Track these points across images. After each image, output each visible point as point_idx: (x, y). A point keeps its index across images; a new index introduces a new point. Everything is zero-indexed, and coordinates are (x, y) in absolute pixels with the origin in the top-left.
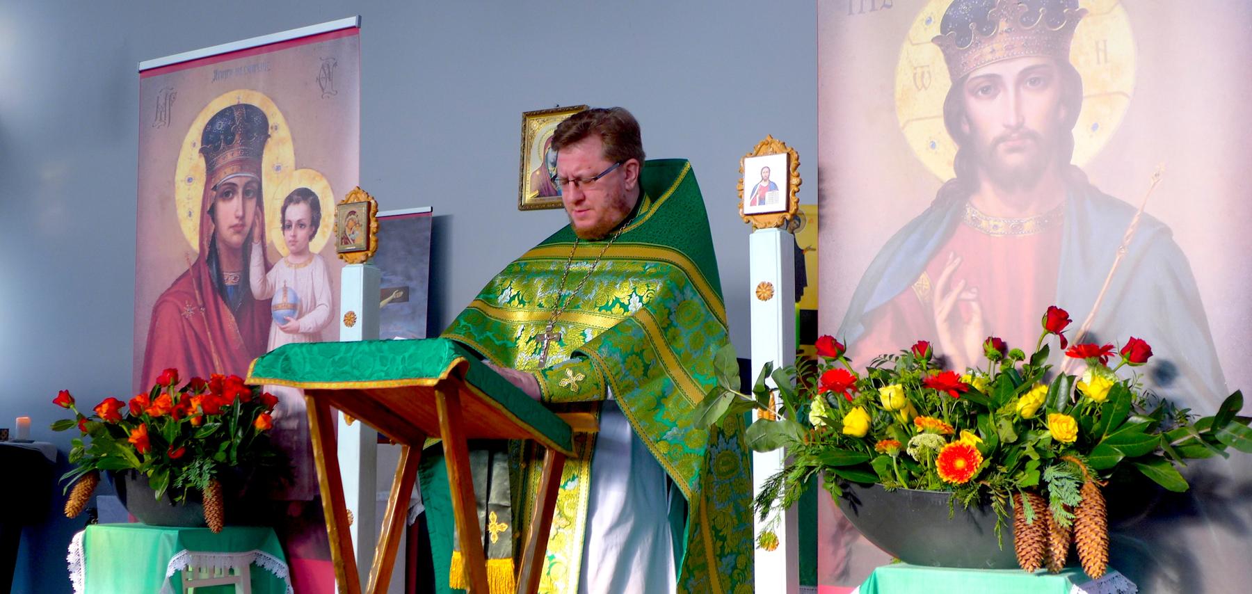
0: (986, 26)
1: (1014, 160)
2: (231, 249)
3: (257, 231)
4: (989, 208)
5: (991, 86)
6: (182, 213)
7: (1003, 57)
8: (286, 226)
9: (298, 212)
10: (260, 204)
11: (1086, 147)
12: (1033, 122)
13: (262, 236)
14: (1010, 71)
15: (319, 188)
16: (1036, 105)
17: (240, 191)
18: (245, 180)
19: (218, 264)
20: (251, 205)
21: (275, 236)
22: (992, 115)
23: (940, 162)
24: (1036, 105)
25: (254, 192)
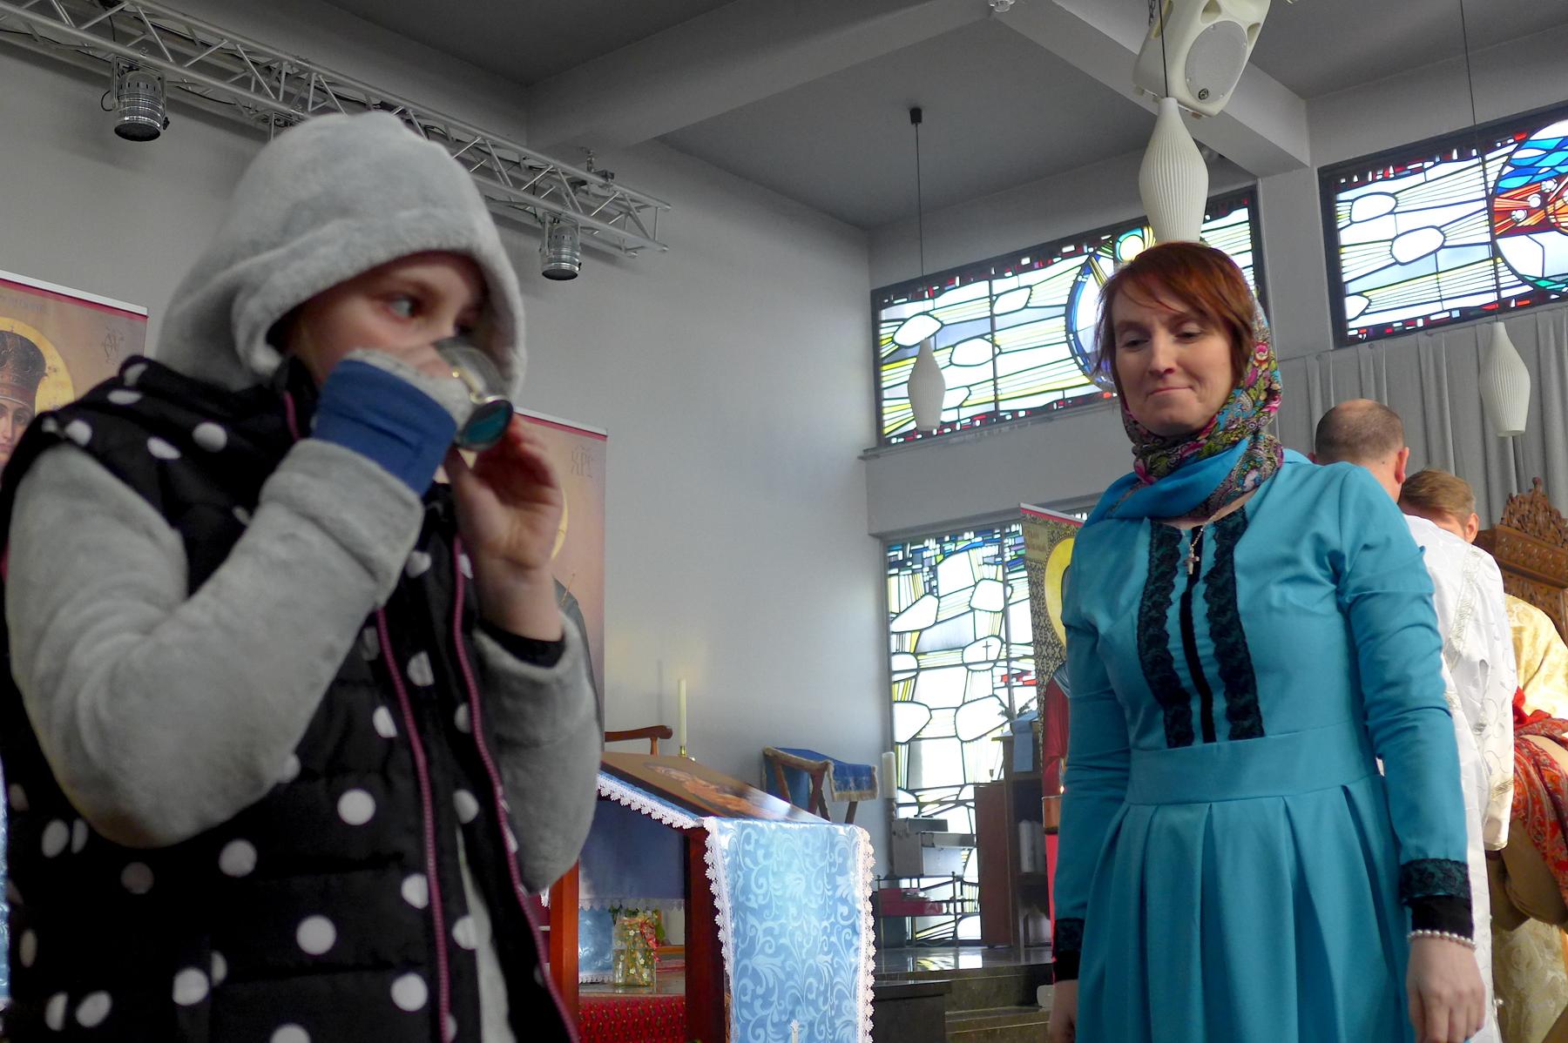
17: (10, 414)
18: (16, 406)
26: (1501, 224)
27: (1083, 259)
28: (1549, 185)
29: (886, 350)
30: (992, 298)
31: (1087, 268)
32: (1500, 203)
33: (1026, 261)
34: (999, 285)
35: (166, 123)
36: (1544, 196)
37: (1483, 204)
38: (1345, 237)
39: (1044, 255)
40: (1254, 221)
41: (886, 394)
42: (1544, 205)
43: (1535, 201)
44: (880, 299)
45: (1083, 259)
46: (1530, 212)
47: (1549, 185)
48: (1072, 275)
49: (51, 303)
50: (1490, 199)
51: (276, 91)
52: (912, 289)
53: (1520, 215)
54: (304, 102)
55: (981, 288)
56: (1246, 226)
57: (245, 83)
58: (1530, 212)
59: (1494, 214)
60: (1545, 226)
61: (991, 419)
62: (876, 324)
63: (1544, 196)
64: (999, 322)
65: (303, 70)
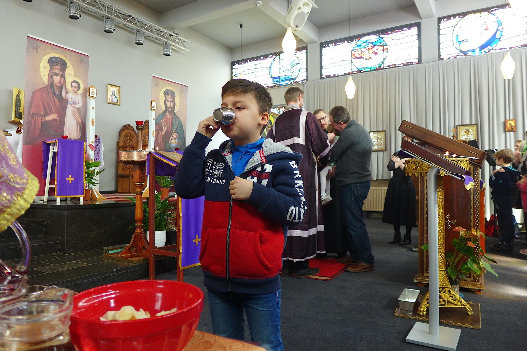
2: (58, 87)
3: (64, 85)
4: (167, 114)
5: (168, 101)
6: (42, 74)
8: (72, 86)
9: (75, 85)
10: (65, 79)
13: (65, 86)
14: (170, 100)
15: (80, 82)
19: (53, 88)
20: (63, 79)
21: (69, 87)
22: (169, 104)
23: (164, 108)
25: (63, 76)
29: (233, 75)
31: (274, 60)
33: (262, 58)
35: (80, 16)
39: (266, 56)
44: (233, 64)
49: (68, 51)
51: (105, 10)
52: (239, 62)
54: (112, 13)
57: (98, 8)
62: (232, 69)
65: (111, 6)
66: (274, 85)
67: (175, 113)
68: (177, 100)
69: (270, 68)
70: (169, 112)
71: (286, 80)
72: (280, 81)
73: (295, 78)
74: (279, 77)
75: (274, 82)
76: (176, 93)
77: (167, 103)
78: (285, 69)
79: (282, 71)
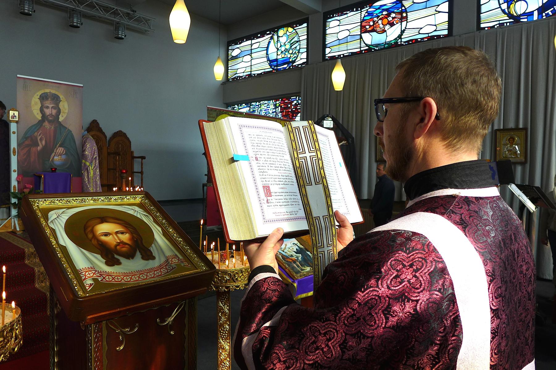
0: (47, 99)
1: (50, 118)
4: (46, 124)
5: (48, 107)
7: (48, 103)
11: (61, 119)
12: (53, 114)
14: (51, 106)
16: (54, 112)
22: (48, 112)
24: (54, 112)
26: (363, 30)
27: (271, 35)
28: (375, 19)
29: (230, 57)
30: (252, 45)
31: (272, 38)
32: (364, 24)
34: (254, 41)
36: (374, 22)
37: (360, 24)
38: (328, 32)
40: (308, 27)
41: (229, 68)
42: (374, 24)
43: (371, 23)
44: (229, 44)
45: (271, 35)
46: (370, 26)
47: (375, 19)
48: (268, 40)
50: (361, 22)
53: (368, 27)
55: (249, 42)
56: (306, 28)
58: (370, 26)
59: (362, 27)
60: (373, 30)
61: (250, 75)
62: (228, 50)
63: (374, 22)
64: (253, 51)
66: (271, 69)
67: (60, 123)
68: (64, 106)
69: (268, 48)
70: (50, 122)
71: (284, 64)
72: (277, 66)
73: (294, 62)
74: (276, 60)
75: (271, 66)
76: (61, 97)
77: (45, 110)
78: (283, 49)
79: (279, 53)
